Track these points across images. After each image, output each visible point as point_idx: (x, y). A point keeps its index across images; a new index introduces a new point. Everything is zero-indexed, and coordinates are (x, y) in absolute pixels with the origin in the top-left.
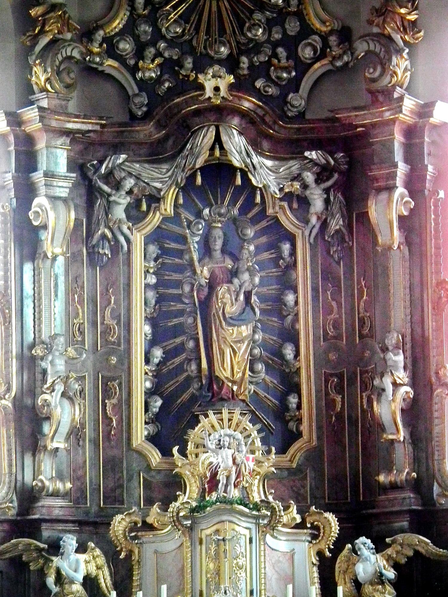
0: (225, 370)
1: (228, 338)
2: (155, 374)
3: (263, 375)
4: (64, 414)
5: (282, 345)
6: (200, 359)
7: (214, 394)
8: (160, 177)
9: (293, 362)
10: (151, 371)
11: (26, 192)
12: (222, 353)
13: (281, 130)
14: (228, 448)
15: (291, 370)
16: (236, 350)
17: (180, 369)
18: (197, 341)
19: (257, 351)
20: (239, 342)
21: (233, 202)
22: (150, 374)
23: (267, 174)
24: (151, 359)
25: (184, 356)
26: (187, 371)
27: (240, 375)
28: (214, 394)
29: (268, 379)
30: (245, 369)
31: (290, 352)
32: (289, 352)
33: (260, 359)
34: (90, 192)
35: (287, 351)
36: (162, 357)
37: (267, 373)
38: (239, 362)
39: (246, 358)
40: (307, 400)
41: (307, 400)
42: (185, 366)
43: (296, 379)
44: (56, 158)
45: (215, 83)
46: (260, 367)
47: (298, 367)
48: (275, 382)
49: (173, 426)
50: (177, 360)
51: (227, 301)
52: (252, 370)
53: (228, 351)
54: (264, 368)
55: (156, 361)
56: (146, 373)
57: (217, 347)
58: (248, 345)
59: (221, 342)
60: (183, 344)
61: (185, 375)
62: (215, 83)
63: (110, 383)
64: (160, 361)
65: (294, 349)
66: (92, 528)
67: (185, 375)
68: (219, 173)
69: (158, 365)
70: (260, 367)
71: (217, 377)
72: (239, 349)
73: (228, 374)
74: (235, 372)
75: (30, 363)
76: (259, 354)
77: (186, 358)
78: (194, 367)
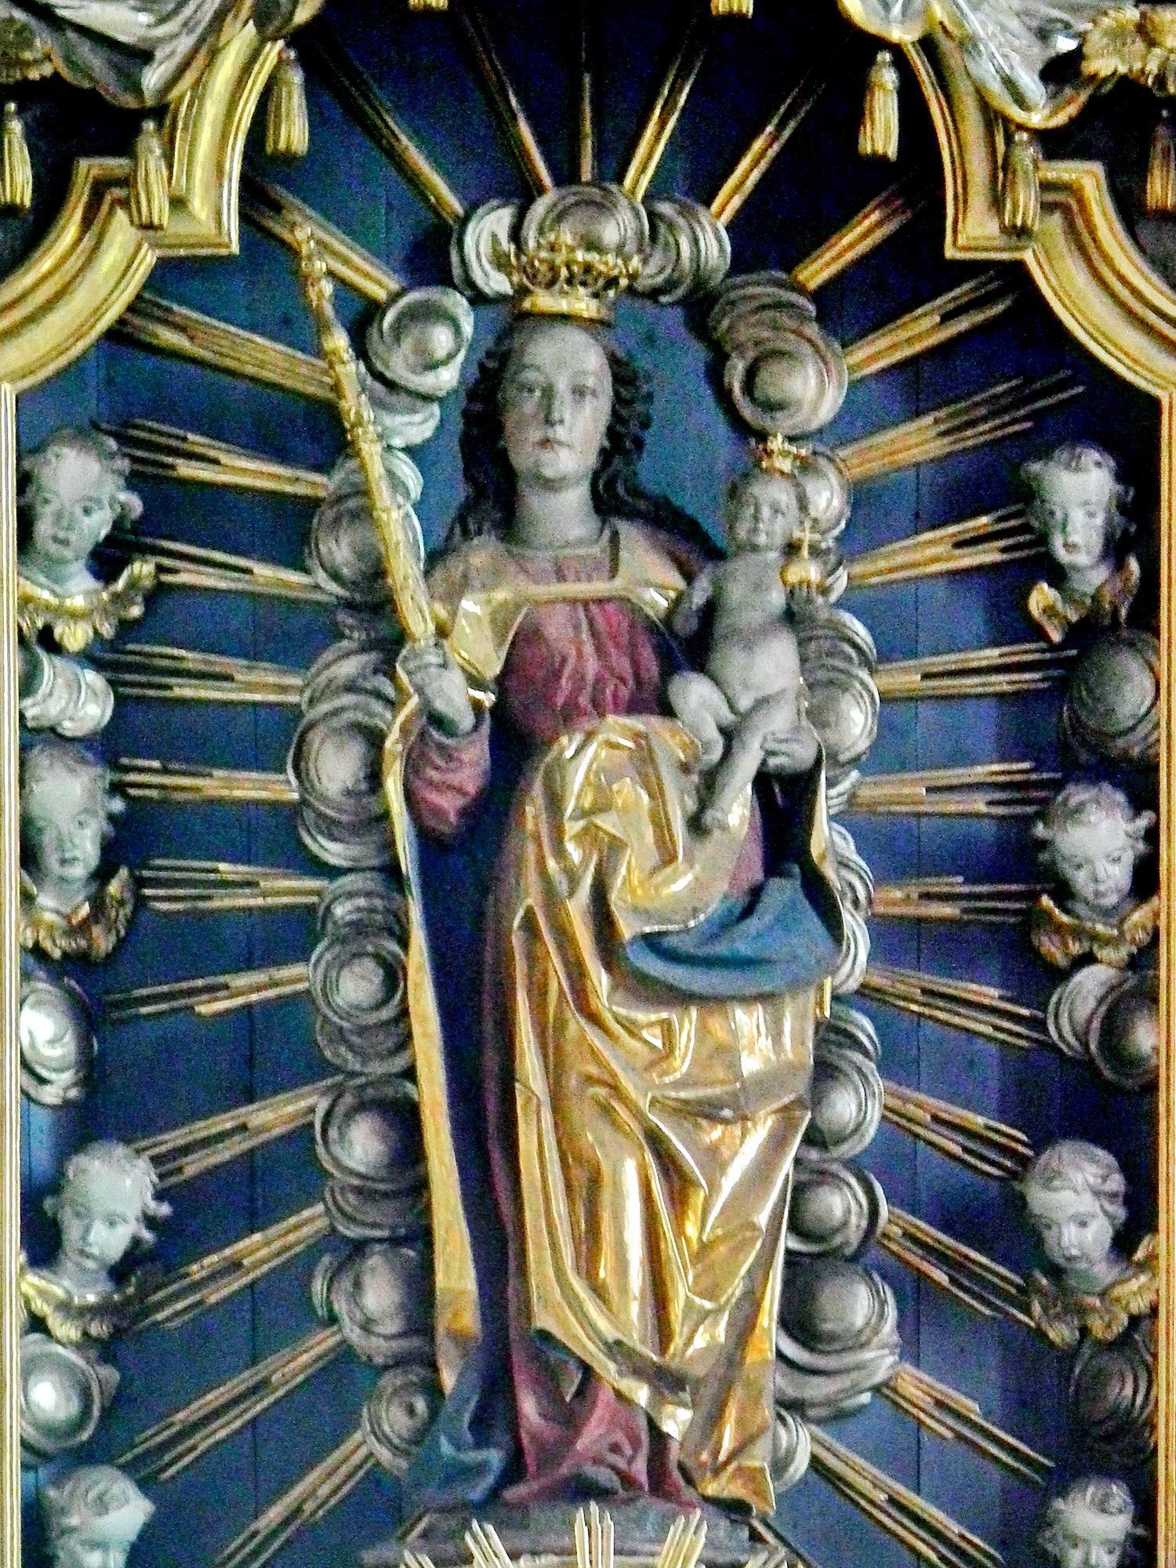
0: (598, 1291)
1: (627, 1083)
2: (97, 1329)
3: (882, 1360)
5: (1024, 1161)
6: (421, 1236)
9: (1104, 1271)
10: (64, 1307)
12: (588, 1189)
15: (1084, 1331)
17: (278, 1306)
18: (405, 1119)
19: (840, 1205)
20: (707, 1111)
21: (697, 172)
22: (66, 1330)
24: (72, 1232)
25: (307, 1223)
26: (333, 1319)
27: (714, 1334)
29: (917, 1385)
30: (752, 1300)
31: (1087, 1204)
32: (1074, 1198)
33: (866, 1256)
35: (1066, 1196)
36: (150, 1221)
37: (911, 1348)
38: (705, 1248)
39: (763, 1219)
42: (318, 1286)
43: (1122, 1392)
46: (858, 1305)
47: (1139, 1305)
48: (972, 1408)
50: (259, 1250)
52: (799, 1322)
53: (629, 1176)
54: (892, 1313)
55: (109, 1241)
56: (37, 1324)
57: (550, 1140)
58: (777, 1143)
59: (583, 1114)
60: (301, 1137)
61: (321, 1343)
64: (136, 1242)
65: (1116, 1183)
67: (321, 1343)
69: (119, 1272)
70: (858, 1305)
71: (545, 1336)
72: (714, 1158)
73: (632, 1320)
74: (676, 1309)
76: (857, 1223)
77: (329, 1240)
78: (380, 1292)
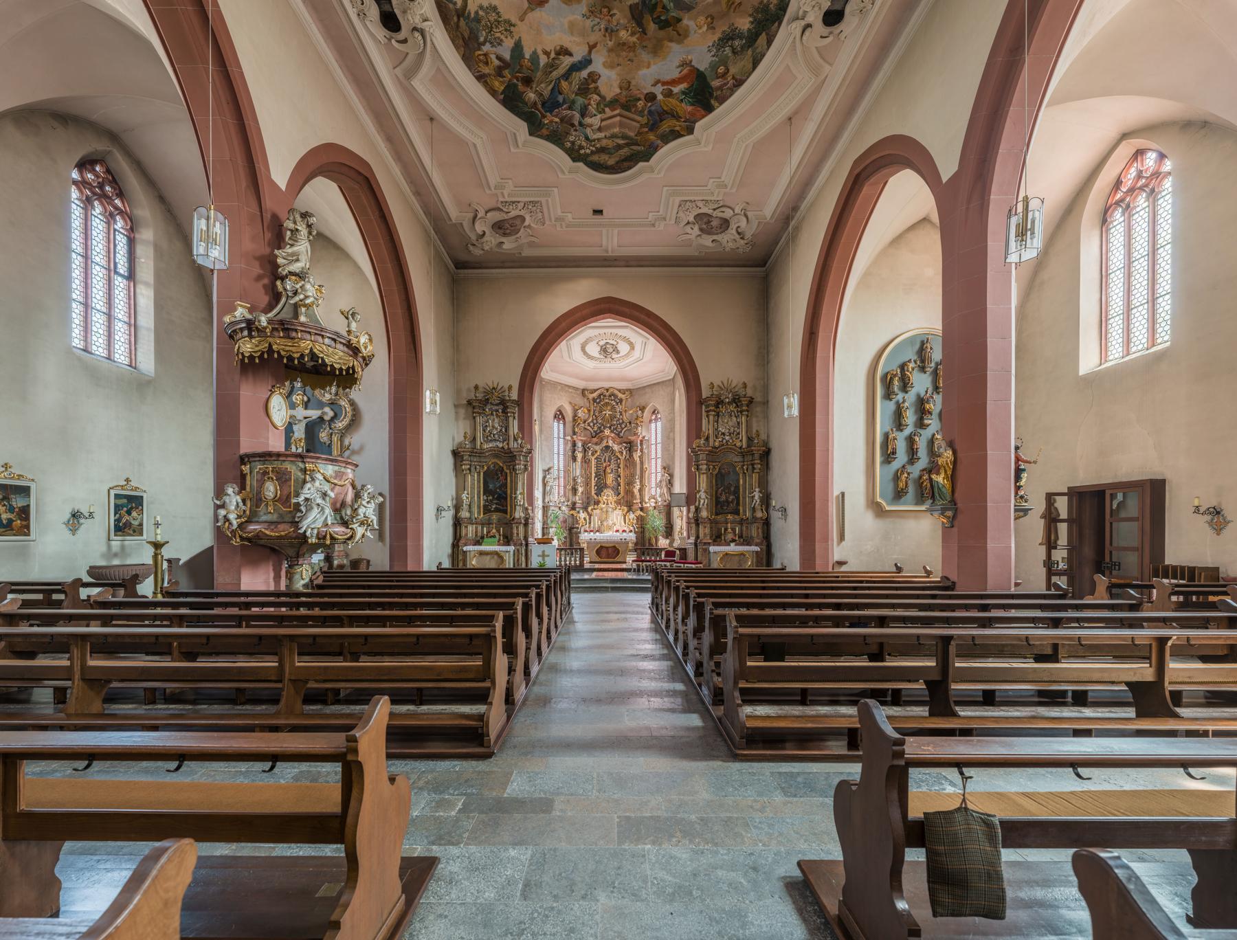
4: (580, 490)
7: (606, 486)
8: (598, 448)
11: (574, 451)
13: (618, 440)
14: (609, 496)
16: (610, 479)
23: (616, 448)
28: (606, 486)
34: (585, 451)
40: (622, 489)
41: (622, 489)
44: (579, 444)
45: (607, 432)
49: (599, 491)
51: (608, 470)
62: (607, 432)
63: (587, 484)
66: (585, 509)
68: (607, 447)
75: (574, 480)
